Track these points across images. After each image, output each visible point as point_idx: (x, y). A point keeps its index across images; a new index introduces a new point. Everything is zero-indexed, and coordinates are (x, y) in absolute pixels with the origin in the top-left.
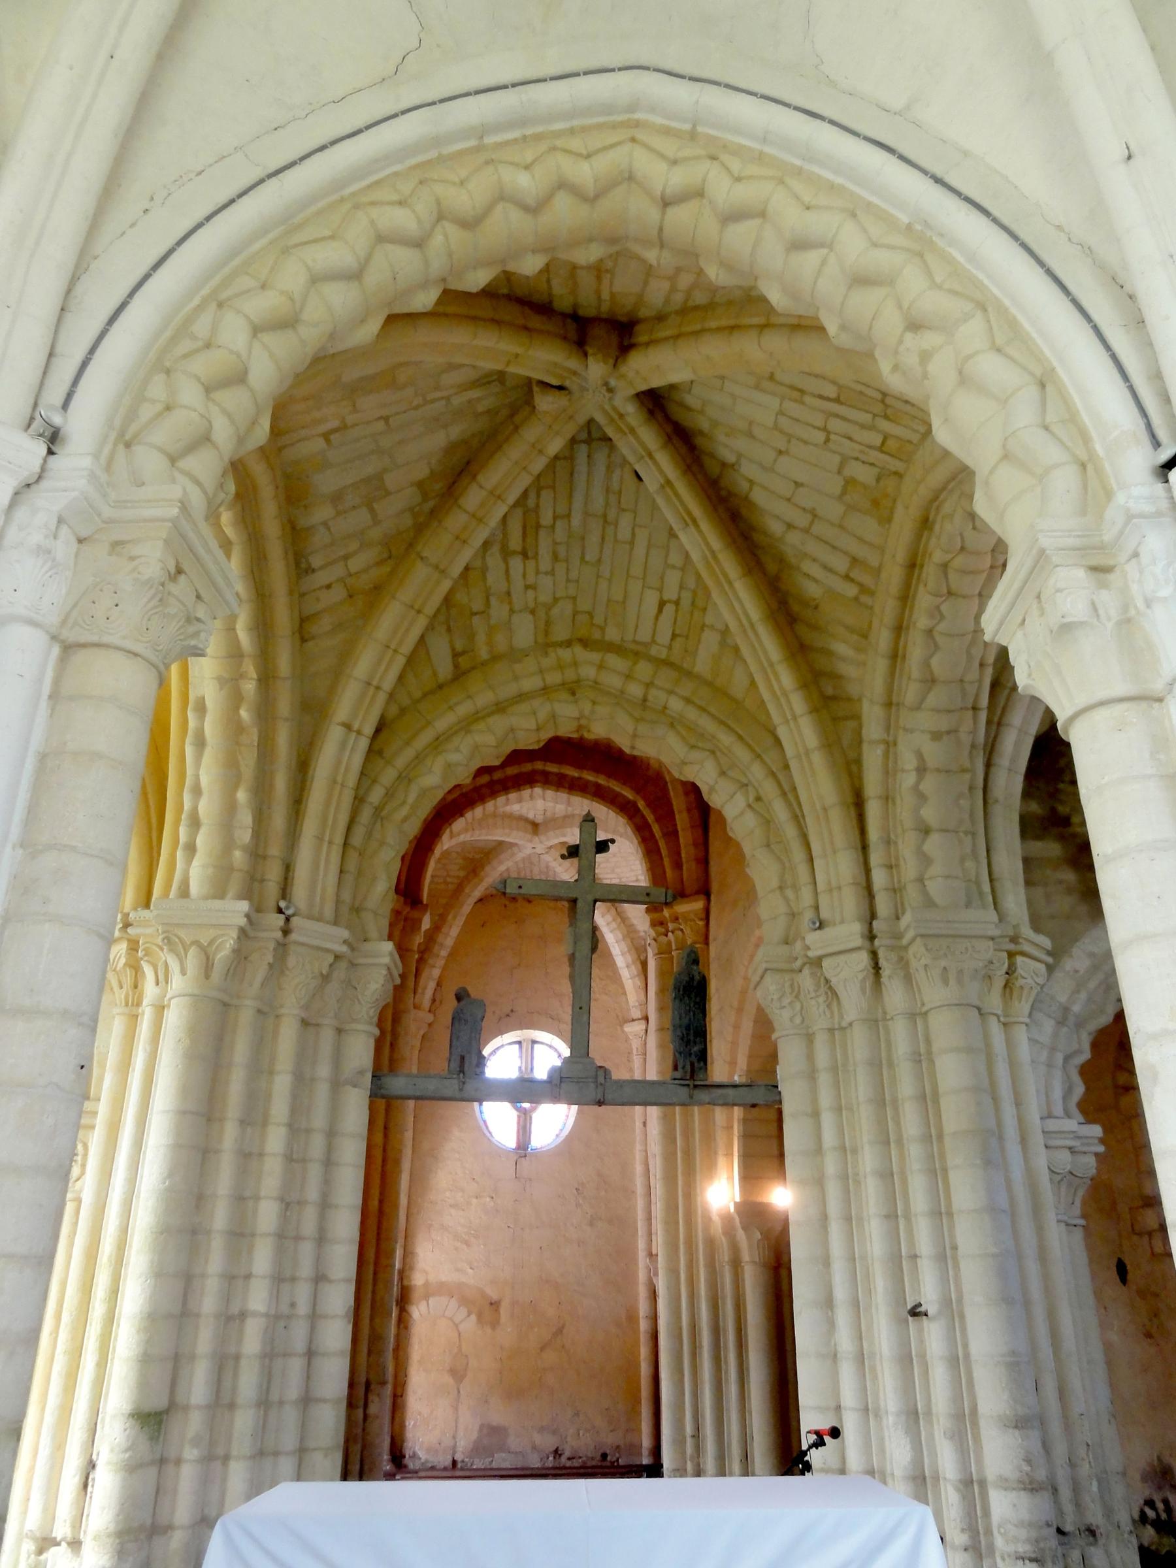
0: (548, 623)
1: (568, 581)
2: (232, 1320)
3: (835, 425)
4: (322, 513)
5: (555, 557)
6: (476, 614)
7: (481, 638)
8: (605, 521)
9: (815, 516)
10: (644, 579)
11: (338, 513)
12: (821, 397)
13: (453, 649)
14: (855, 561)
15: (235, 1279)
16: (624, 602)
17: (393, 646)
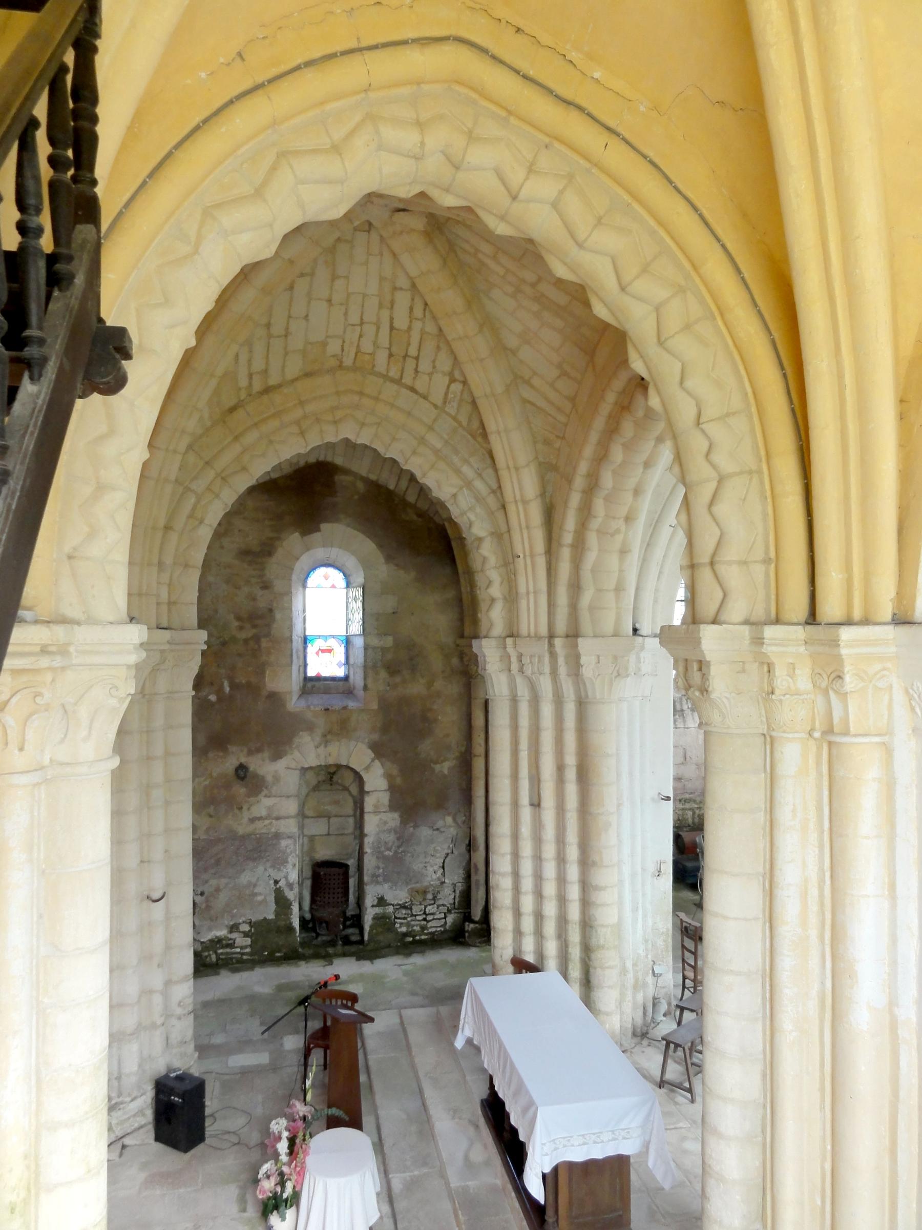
3: (370, 330)
9: (286, 336)
12: (392, 319)
14: (266, 371)
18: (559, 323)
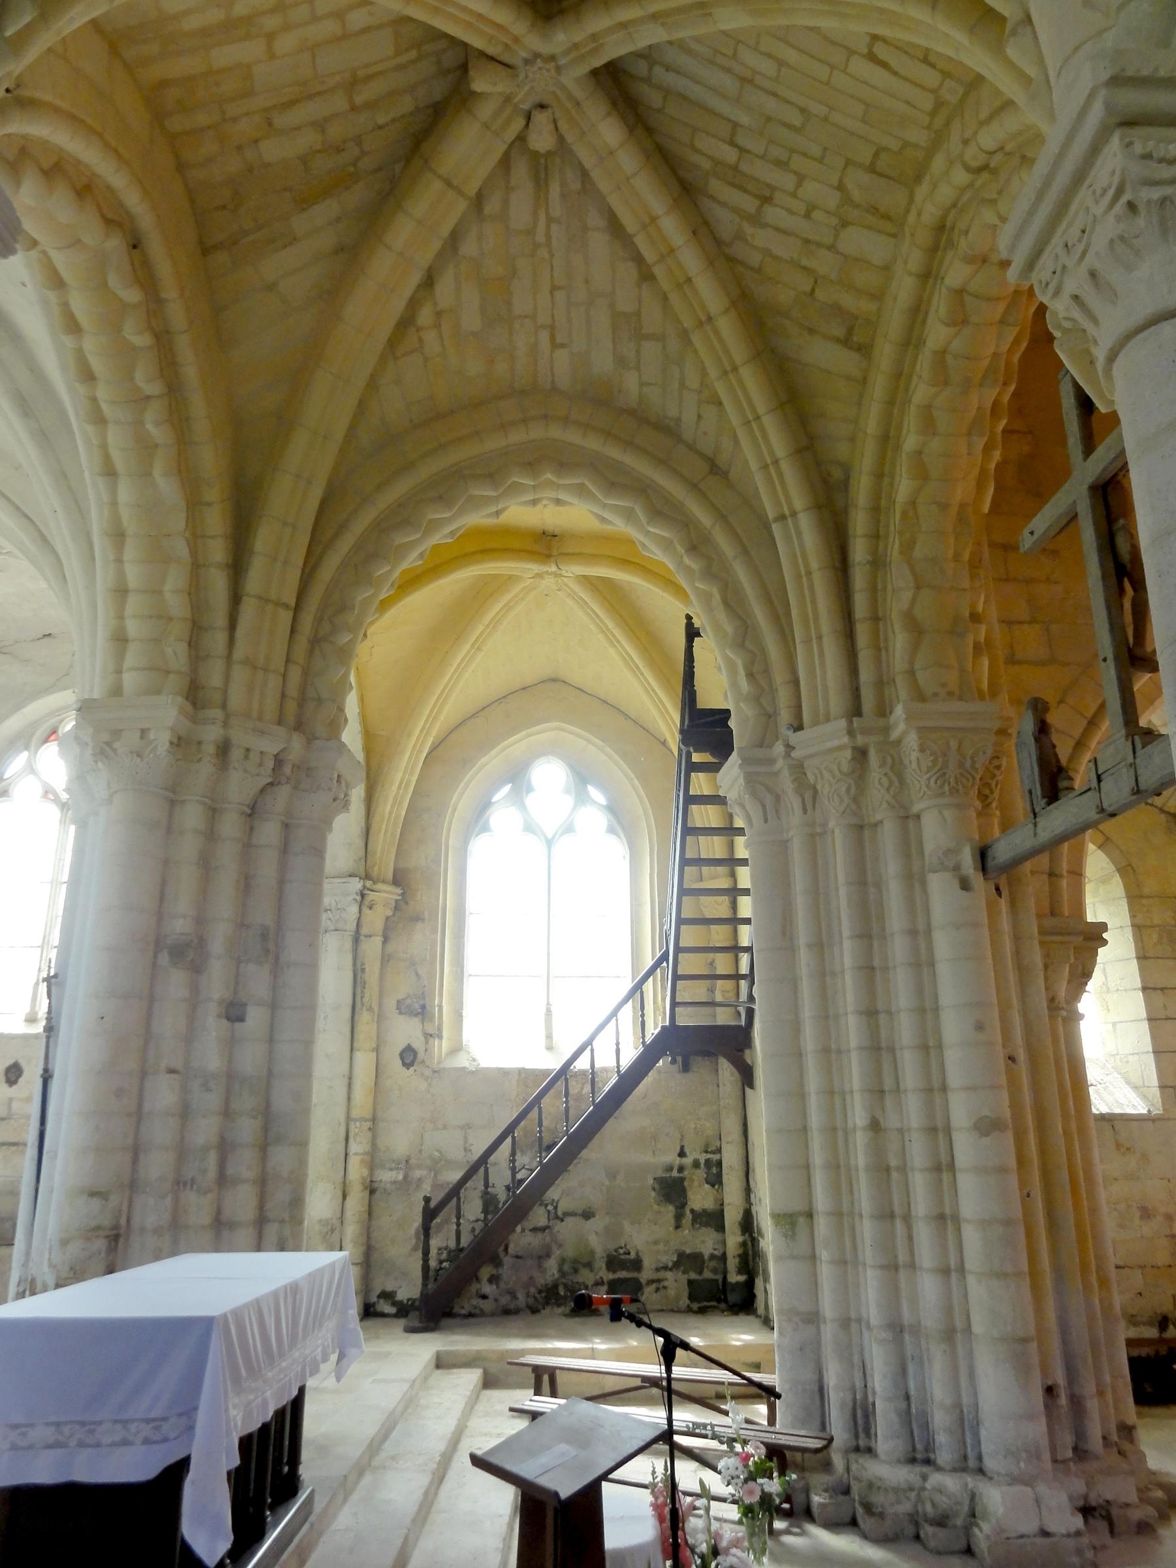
0: (874, 210)
1: (820, 160)
2: (836, 1132)
4: (631, 381)
5: (781, 164)
6: (813, 290)
7: (848, 301)
8: (751, 81)
10: (832, 67)
11: (638, 368)
13: (837, 340)
15: (833, 1094)
16: (867, 105)
17: (751, 418)
18: (192, 23)
